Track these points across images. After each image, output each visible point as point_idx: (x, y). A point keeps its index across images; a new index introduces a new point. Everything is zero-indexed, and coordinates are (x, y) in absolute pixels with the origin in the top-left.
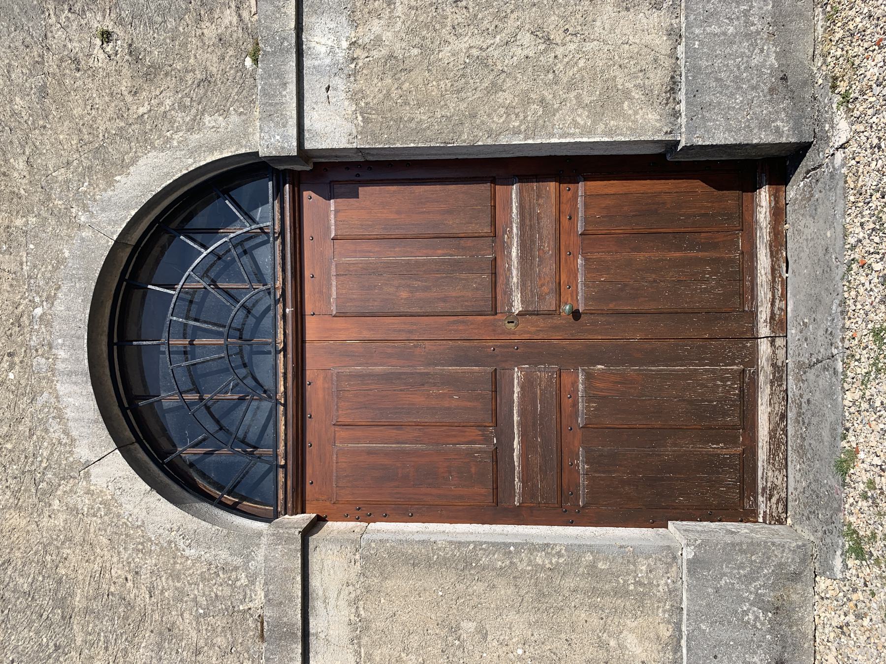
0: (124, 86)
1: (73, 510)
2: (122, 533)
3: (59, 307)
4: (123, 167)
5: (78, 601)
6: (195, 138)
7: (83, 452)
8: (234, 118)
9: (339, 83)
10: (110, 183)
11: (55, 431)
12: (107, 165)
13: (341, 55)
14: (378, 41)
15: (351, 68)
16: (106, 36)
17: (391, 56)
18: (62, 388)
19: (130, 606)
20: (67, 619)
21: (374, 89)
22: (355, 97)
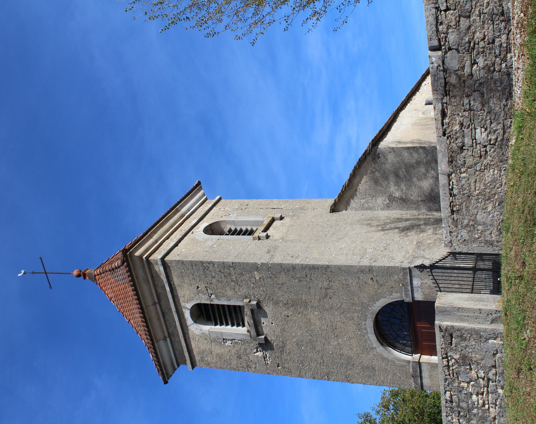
0: (376, 287)
1: (374, 355)
2: (383, 359)
3: (367, 322)
4: (377, 300)
5: (377, 368)
6: (391, 297)
7: (374, 346)
8: (399, 294)
9: (419, 289)
10: (375, 303)
11: (369, 342)
12: (374, 299)
13: (419, 285)
14: (427, 283)
15: (422, 286)
16: (372, 279)
17: (429, 286)
18: (369, 335)
19: (387, 370)
20: (375, 371)
21: (427, 291)
22: (423, 292)
